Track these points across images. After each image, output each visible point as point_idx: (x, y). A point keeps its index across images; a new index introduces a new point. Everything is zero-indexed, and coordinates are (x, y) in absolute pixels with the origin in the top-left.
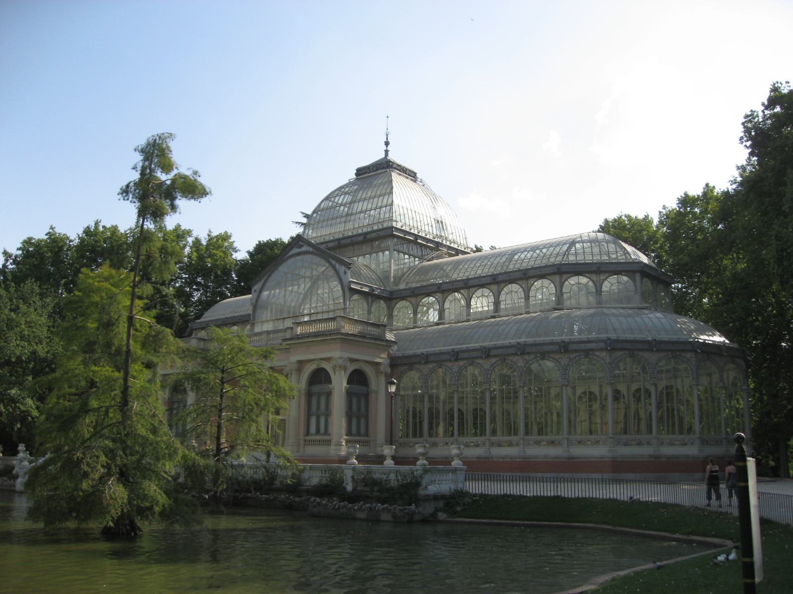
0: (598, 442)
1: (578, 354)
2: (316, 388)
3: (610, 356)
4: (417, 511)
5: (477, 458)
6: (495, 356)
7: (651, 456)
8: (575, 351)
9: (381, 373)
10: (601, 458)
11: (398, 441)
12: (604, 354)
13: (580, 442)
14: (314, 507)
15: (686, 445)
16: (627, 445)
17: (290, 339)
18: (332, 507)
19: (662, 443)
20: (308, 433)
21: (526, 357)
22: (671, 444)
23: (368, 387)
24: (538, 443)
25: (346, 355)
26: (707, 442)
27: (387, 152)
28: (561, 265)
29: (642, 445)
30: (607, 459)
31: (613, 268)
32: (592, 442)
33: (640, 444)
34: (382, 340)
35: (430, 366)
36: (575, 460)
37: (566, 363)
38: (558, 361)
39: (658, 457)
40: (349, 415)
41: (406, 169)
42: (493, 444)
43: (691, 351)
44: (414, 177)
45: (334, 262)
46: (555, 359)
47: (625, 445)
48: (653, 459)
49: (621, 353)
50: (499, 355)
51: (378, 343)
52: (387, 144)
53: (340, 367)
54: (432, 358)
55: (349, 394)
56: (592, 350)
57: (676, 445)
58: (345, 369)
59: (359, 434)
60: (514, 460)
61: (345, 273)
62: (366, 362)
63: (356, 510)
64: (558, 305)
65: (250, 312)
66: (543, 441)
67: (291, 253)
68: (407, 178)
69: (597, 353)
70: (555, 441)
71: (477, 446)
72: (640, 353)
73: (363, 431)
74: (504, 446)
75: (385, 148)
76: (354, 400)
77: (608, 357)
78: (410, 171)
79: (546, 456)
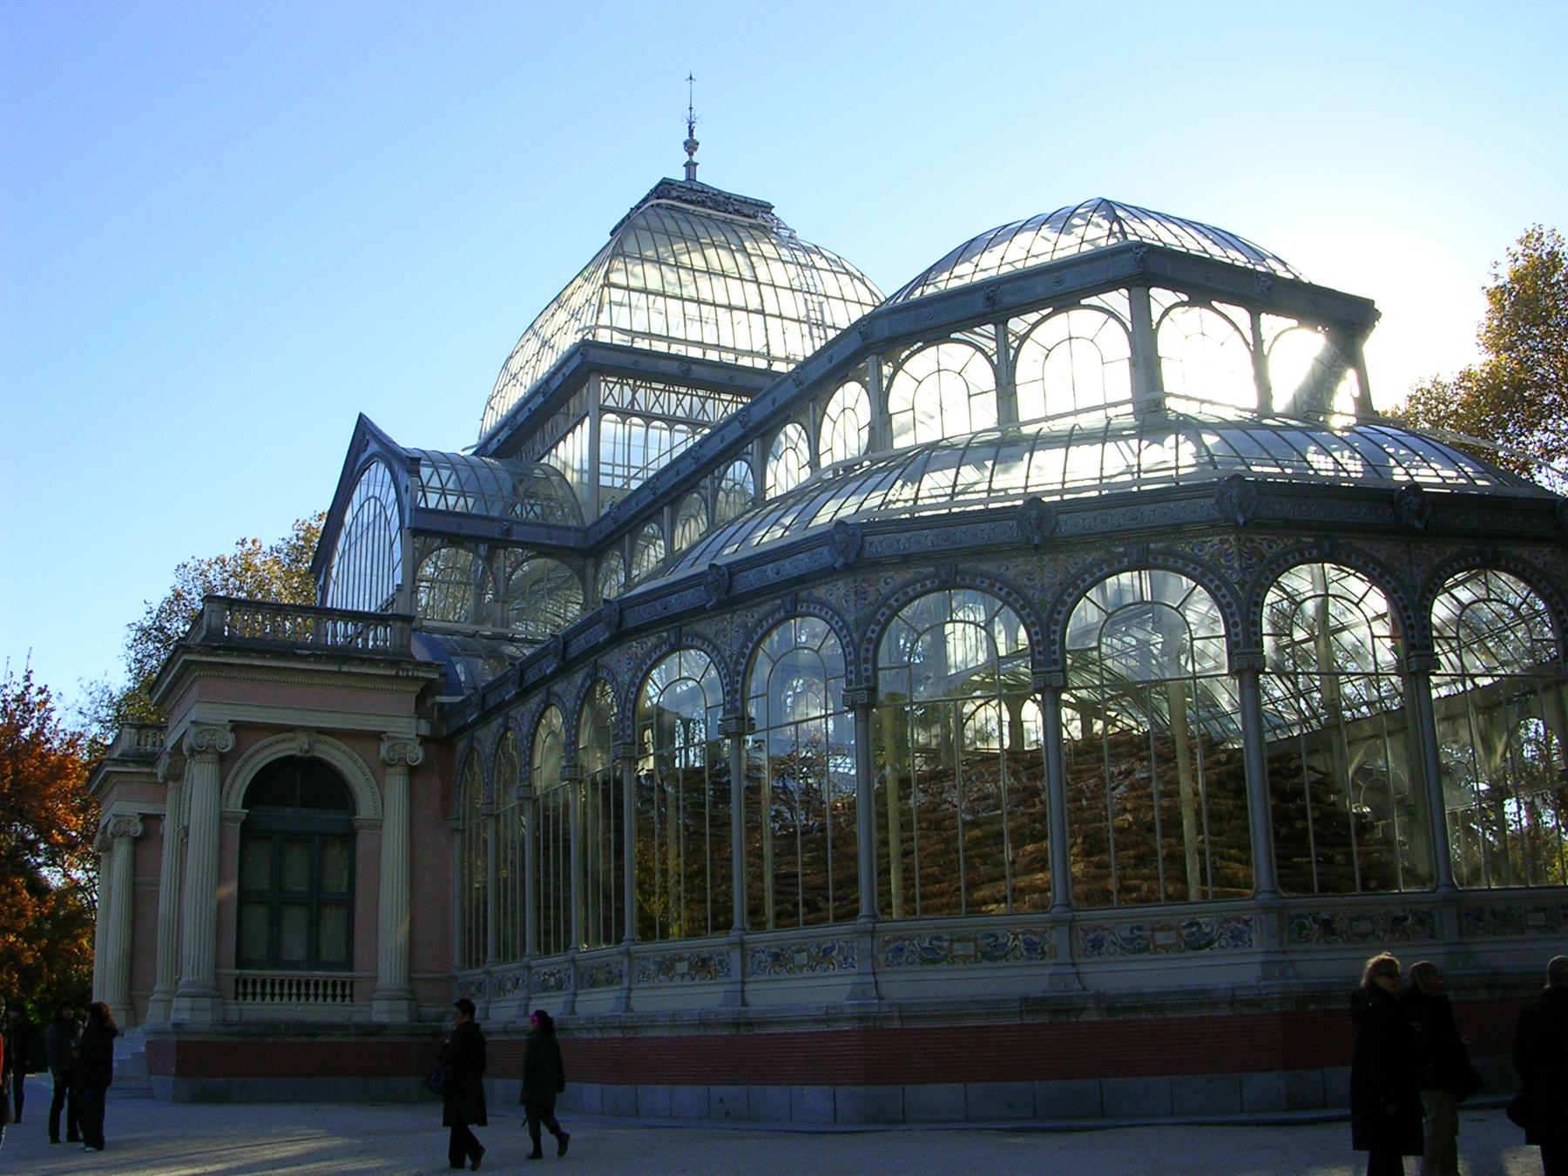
0: (827, 952)
1: (767, 607)
3: (861, 594)
7: (1029, 1004)
10: (828, 1020)
12: (836, 592)
15: (1210, 944)
16: (933, 962)
19: (1097, 945)
21: (635, 647)
22: (1138, 945)
23: (354, 813)
27: (690, 166)
30: (846, 1026)
33: (993, 952)
36: (758, 1031)
38: (715, 647)
39: (1055, 1006)
45: (396, 466)
47: (923, 961)
48: (1044, 1019)
49: (908, 575)
51: (353, 670)
52: (691, 146)
56: (801, 580)
57: (1167, 948)
58: (224, 760)
59: (314, 961)
66: (681, 959)
75: (688, 158)
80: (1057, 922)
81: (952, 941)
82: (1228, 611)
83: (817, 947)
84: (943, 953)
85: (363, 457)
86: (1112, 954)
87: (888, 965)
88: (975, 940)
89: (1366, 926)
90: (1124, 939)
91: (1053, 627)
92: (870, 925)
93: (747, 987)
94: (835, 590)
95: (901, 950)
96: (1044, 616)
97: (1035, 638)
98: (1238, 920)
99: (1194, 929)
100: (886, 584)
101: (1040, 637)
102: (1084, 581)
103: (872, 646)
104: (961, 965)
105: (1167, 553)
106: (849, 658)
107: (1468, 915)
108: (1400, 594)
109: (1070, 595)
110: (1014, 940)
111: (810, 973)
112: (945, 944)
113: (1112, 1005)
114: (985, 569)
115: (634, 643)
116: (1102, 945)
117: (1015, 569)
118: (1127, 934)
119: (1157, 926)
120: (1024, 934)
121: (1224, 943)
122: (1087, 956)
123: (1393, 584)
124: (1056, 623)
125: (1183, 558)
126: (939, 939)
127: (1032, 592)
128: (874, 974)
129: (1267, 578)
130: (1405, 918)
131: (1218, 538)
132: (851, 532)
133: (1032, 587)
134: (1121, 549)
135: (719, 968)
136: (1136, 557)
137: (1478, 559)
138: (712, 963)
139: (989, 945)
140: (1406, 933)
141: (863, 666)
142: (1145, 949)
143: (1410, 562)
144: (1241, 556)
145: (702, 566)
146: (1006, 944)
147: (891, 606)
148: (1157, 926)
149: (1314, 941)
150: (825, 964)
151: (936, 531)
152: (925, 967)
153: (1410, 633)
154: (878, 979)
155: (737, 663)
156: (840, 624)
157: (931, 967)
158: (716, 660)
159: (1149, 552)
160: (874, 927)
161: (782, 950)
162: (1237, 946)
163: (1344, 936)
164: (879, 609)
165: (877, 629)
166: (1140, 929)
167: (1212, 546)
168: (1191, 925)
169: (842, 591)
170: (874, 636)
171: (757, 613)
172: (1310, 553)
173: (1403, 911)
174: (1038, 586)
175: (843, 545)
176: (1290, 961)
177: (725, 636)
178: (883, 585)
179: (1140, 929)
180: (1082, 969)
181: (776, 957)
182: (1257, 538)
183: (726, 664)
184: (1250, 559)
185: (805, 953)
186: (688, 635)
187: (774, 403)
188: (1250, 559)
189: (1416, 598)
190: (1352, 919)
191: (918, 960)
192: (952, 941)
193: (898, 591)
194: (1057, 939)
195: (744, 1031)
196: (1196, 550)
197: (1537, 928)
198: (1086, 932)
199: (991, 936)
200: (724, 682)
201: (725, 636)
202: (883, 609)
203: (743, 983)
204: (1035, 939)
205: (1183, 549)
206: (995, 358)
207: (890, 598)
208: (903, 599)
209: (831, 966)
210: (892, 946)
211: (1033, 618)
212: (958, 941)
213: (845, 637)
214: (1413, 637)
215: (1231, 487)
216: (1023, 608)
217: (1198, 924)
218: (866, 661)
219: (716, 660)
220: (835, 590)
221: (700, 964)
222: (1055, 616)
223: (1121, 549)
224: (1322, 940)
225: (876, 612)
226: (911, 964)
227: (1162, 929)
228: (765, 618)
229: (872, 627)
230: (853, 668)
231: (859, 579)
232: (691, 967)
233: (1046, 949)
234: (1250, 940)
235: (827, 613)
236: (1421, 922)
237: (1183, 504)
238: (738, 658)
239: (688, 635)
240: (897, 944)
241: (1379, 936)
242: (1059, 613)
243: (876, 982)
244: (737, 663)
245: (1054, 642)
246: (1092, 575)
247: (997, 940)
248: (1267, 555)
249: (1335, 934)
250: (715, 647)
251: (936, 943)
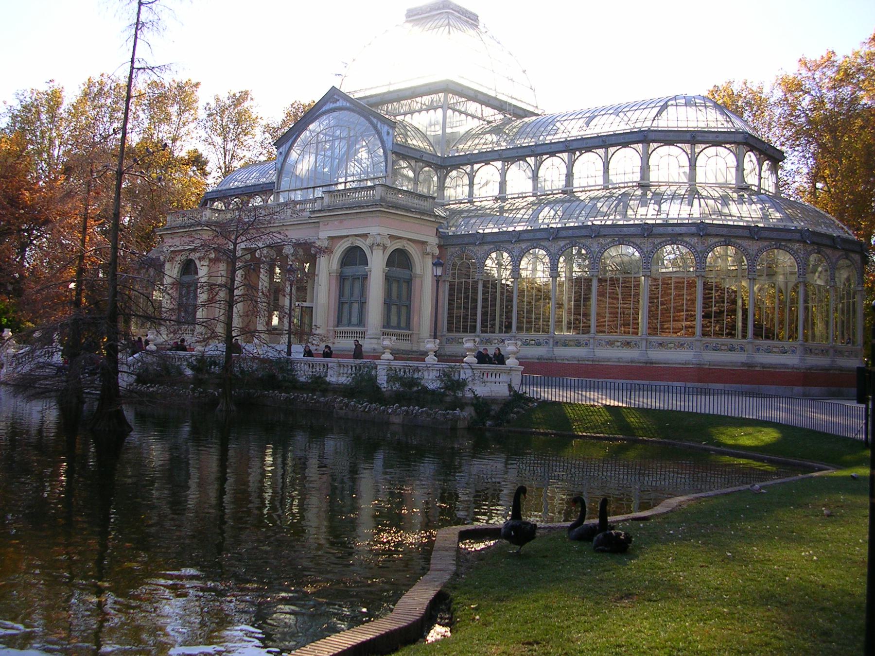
1: (664, 239)
2: (349, 271)
4: (462, 416)
5: (538, 359)
6: (565, 238)
8: (661, 235)
9: (428, 254)
11: (445, 335)
12: (695, 240)
13: (661, 344)
14: (341, 409)
17: (320, 211)
18: (362, 409)
19: (758, 350)
20: (339, 322)
21: (601, 240)
22: (769, 351)
24: (611, 343)
25: (385, 231)
26: (811, 350)
28: (649, 131)
31: (711, 137)
32: (675, 345)
33: (732, 349)
34: (430, 215)
35: (486, 247)
39: (750, 365)
40: (388, 303)
41: (467, 11)
42: (557, 342)
43: (798, 241)
44: (475, 21)
45: (375, 121)
46: (637, 245)
47: (714, 350)
49: (717, 240)
50: (569, 237)
53: (378, 245)
54: (489, 239)
55: (388, 278)
58: (385, 248)
59: (398, 327)
60: (581, 362)
61: (388, 133)
62: (409, 240)
63: (390, 414)
64: (642, 178)
65: (274, 179)
67: (324, 109)
68: (467, 22)
69: (687, 239)
71: (539, 344)
73: (403, 324)
74: (571, 346)
76: (395, 286)
78: (471, 13)
79: (619, 360)
80: (749, 343)
85: (332, 106)
89: (817, 352)
105: (785, 246)
113: (763, 366)
117: (745, 243)
194: (748, 347)
195: (648, 365)
206: (690, 155)
228: (663, 242)
232: (622, 344)
239: (626, 241)
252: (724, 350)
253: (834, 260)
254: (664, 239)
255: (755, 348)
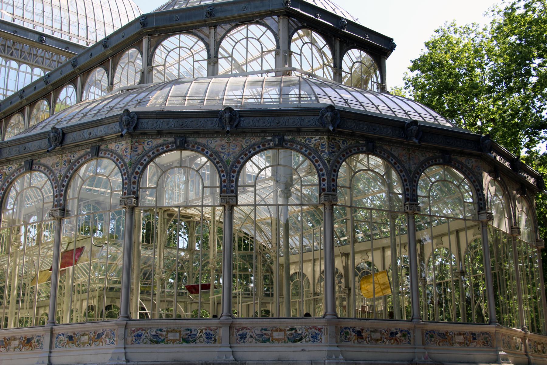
0: (99, 336)
1: (82, 152)
3: (134, 149)
15: (300, 340)
16: (157, 342)
19: (243, 337)
29: (194, 341)
37: (63, 172)
38: (51, 172)
43: (317, 132)
47: (152, 342)
49: (160, 141)
56: (102, 140)
57: (278, 340)
66: (15, 339)
69: (112, 146)
70: (32, 338)
72: (200, 140)
77: (129, 150)
80: (223, 324)
81: (168, 332)
82: (321, 173)
83: (95, 333)
84: (162, 338)
86: (251, 342)
87: (132, 344)
88: (180, 331)
89: (377, 335)
90: (257, 335)
91: (232, 174)
92: (125, 322)
93: (52, 355)
94: (120, 146)
95: (140, 335)
96: (229, 168)
97: (223, 179)
98: (315, 328)
99: (293, 332)
100: (148, 145)
101: (225, 178)
102: (250, 152)
103: (138, 176)
104: (171, 345)
106: (125, 182)
107: (427, 334)
108: (403, 173)
109: (242, 158)
110: (200, 332)
111: (89, 348)
112: (164, 333)
114: (200, 141)
115: (5, 167)
116: (246, 338)
117: (215, 143)
118: (259, 332)
119: (274, 329)
120: (206, 329)
121: (308, 339)
122: (237, 343)
123: (401, 168)
124: (234, 172)
125: (300, 145)
126: (161, 330)
127: (223, 155)
128: (125, 348)
129: (341, 159)
130: (397, 333)
131: (319, 137)
132: (132, 116)
133: (224, 153)
134: (270, 138)
135: (37, 344)
136: (277, 142)
137: (441, 160)
138: (33, 341)
139: (187, 334)
140: (397, 340)
141: (132, 186)
142: (267, 340)
143: (409, 159)
144: (329, 147)
145: (49, 128)
146: (196, 335)
147: (149, 156)
148: (274, 329)
149: (352, 342)
150: (98, 343)
151: (177, 120)
152: (152, 345)
153: (407, 192)
154: (127, 350)
155: (63, 181)
156: (122, 163)
157: (156, 345)
158: (51, 179)
159: (284, 140)
160: (127, 323)
161: (74, 334)
162: (314, 341)
163: (367, 340)
164: (144, 156)
165: (141, 167)
166: (265, 330)
167: (315, 140)
168: (291, 329)
169: (124, 147)
170: (139, 171)
171: (77, 155)
172: (362, 149)
173: (396, 329)
174: (227, 152)
175: (127, 122)
176: (341, 351)
177: (57, 166)
178: (146, 144)
179: (265, 330)
180: (234, 350)
181: (70, 338)
182: (338, 139)
183: (57, 181)
184: (333, 148)
185: (87, 336)
186: (37, 164)
187: (91, 56)
188: (333, 148)
189: (411, 176)
190: (371, 331)
191: (149, 342)
192: (168, 332)
193: (154, 148)
194: (223, 333)
196: (307, 142)
197: (460, 343)
198: (238, 331)
199: (188, 330)
200: (55, 190)
201: (57, 166)
202: (146, 157)
203: (50, 352)
204: (212, 333)
205: (301, 141)
207: (149, 152)
208: (156, 153)
209: (101, 344)
210: (136, 333)
211: (223, 168)
212: (172, 332)
213: (124, 170)
214: (408, 195)
215: (327, 112)
216: (218, 163)
217: (295, 329)
218: (134, 183)
219: (51, 179)
220: (120, 146)
221: (26, 341)
222: (234, 168)
223: (270, 138)
224: (356, 341)
225: (141, 159)
226: (145, 343)
227: (277, 331)
228: (81, 158)
229: (139, 166)
230: (127, 186)
231: (134, 141)
232: (20, 343)
233: (217, 338)
234: (321, 339)
235: (115, 157)
236: (404, 336)
237: (303, 118)
238: (64, 177)
239: (37, 164)
240: (138, 332)
241: (384, 341)
242: (236, 167)
243: (125, 353)
244: (63, 181)
245: (232, 181)
246: (254, 149)
247: (191, 332)
248: (342, 147)
249: (363, 339)
250: (51, 172)
251: (159, 332)
252: (174, 341)
253: (413, 168)
254: (82, 152)
255: (236, 335)
